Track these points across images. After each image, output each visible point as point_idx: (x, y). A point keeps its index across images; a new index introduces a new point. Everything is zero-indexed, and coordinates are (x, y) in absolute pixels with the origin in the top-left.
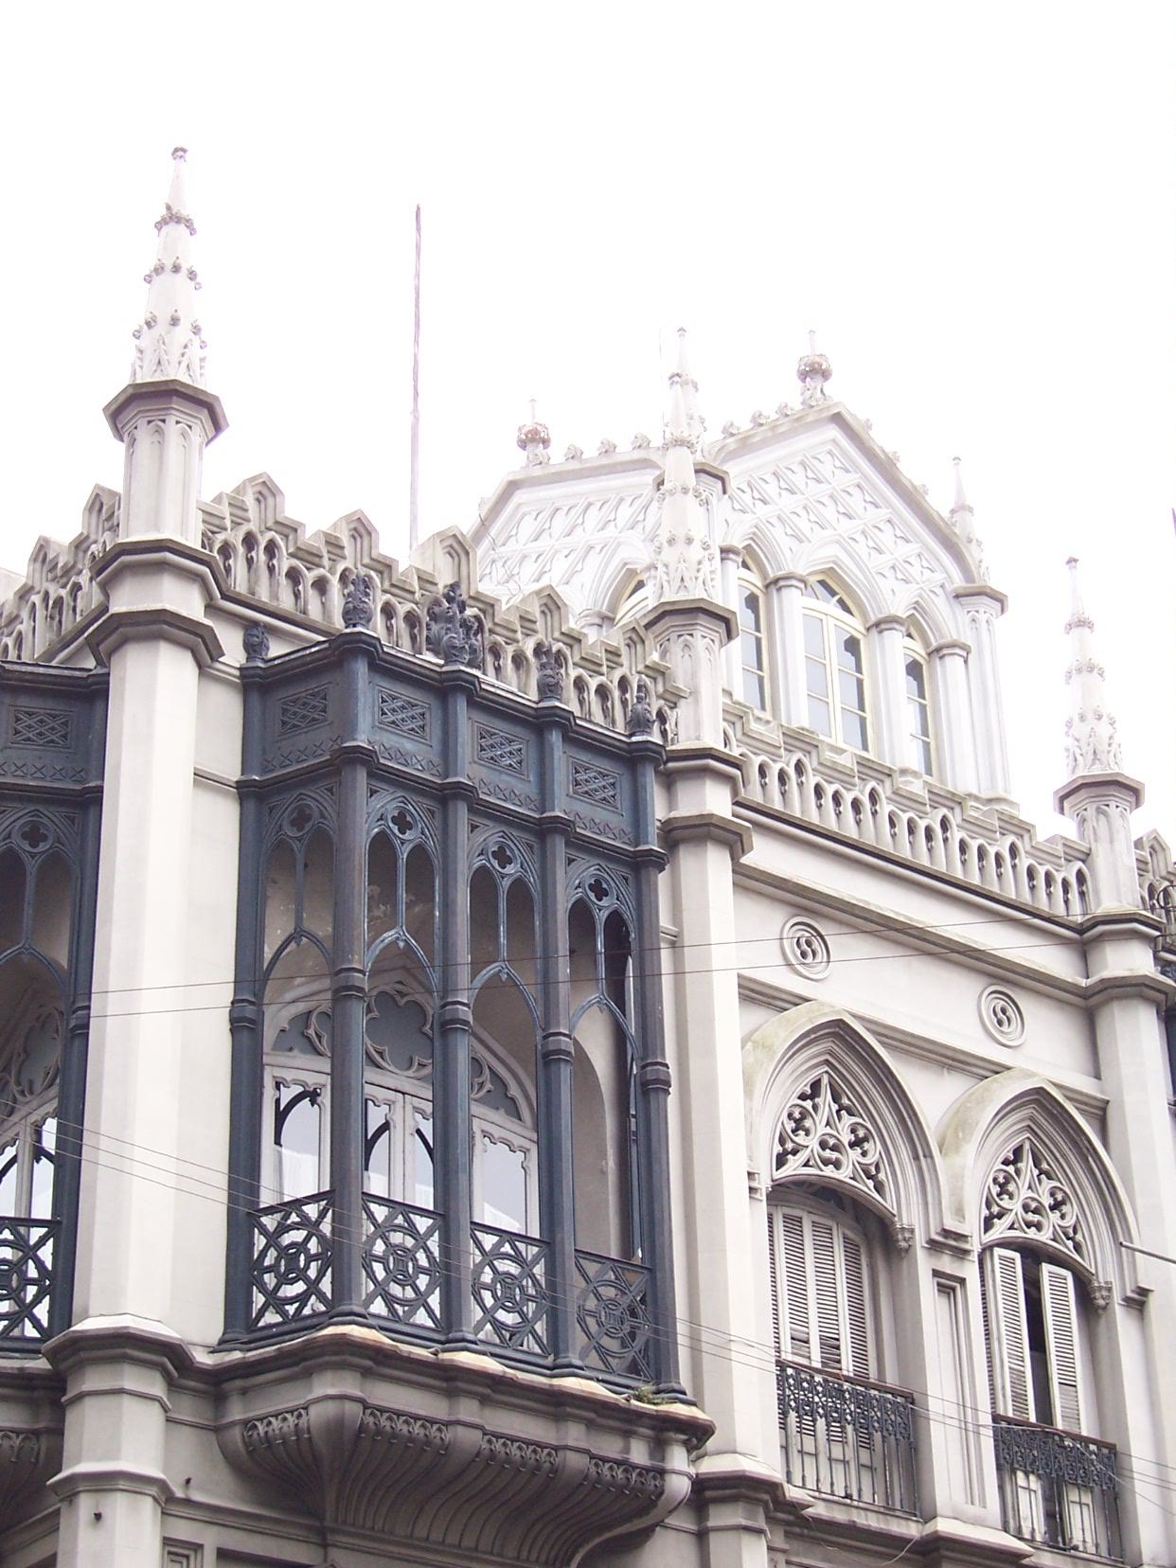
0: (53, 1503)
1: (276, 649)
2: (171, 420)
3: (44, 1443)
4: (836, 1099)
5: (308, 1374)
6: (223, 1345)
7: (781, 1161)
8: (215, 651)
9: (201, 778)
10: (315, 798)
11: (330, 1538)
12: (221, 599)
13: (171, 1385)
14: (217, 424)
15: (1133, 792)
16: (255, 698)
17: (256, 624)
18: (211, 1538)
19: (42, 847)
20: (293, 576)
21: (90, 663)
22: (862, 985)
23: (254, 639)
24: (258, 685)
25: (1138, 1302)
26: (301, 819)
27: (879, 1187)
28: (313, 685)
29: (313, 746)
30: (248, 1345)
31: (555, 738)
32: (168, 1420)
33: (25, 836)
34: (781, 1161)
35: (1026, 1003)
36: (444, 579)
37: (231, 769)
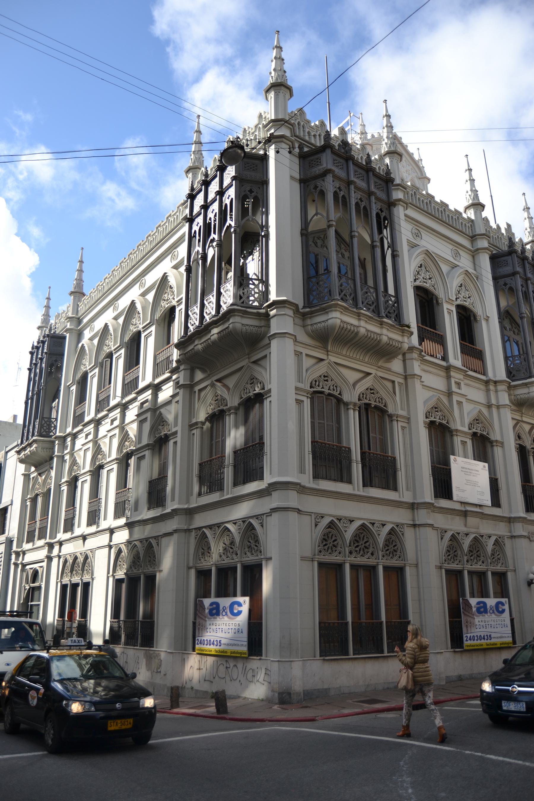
0: (266, 341)
1: (306, 149)
2: (281, 92)
3: (263, 329)
4: (426, 268)
5: (327, 313)
6: (304, 307)
7: (415, 280)
8: (294, 148)
9: (292, 178)
10: (319, 183)
11: (329, 353)
12: (294, 134)
13: (294, 313)
14: (291, 95)
15: (483, 206)
16: (301, 160)
17: (301, 143)
18: (305, 351)
19: (253, 194)
20: (309, 133)
21: (262, 152)
22: (429, 242)
23: (301, 147)
24: (303, 157)
25: (487, 319)
26: (316, 187)
27: (435, 288)
28: (316, 156)
29: (317, 170)
30: (310, 307)
31: (371, 174)
32: (294, 324)
33: (249, 191)
34: (415, 280)
35: (461, 253)
36: (341, 139)
37: (297, 176)
